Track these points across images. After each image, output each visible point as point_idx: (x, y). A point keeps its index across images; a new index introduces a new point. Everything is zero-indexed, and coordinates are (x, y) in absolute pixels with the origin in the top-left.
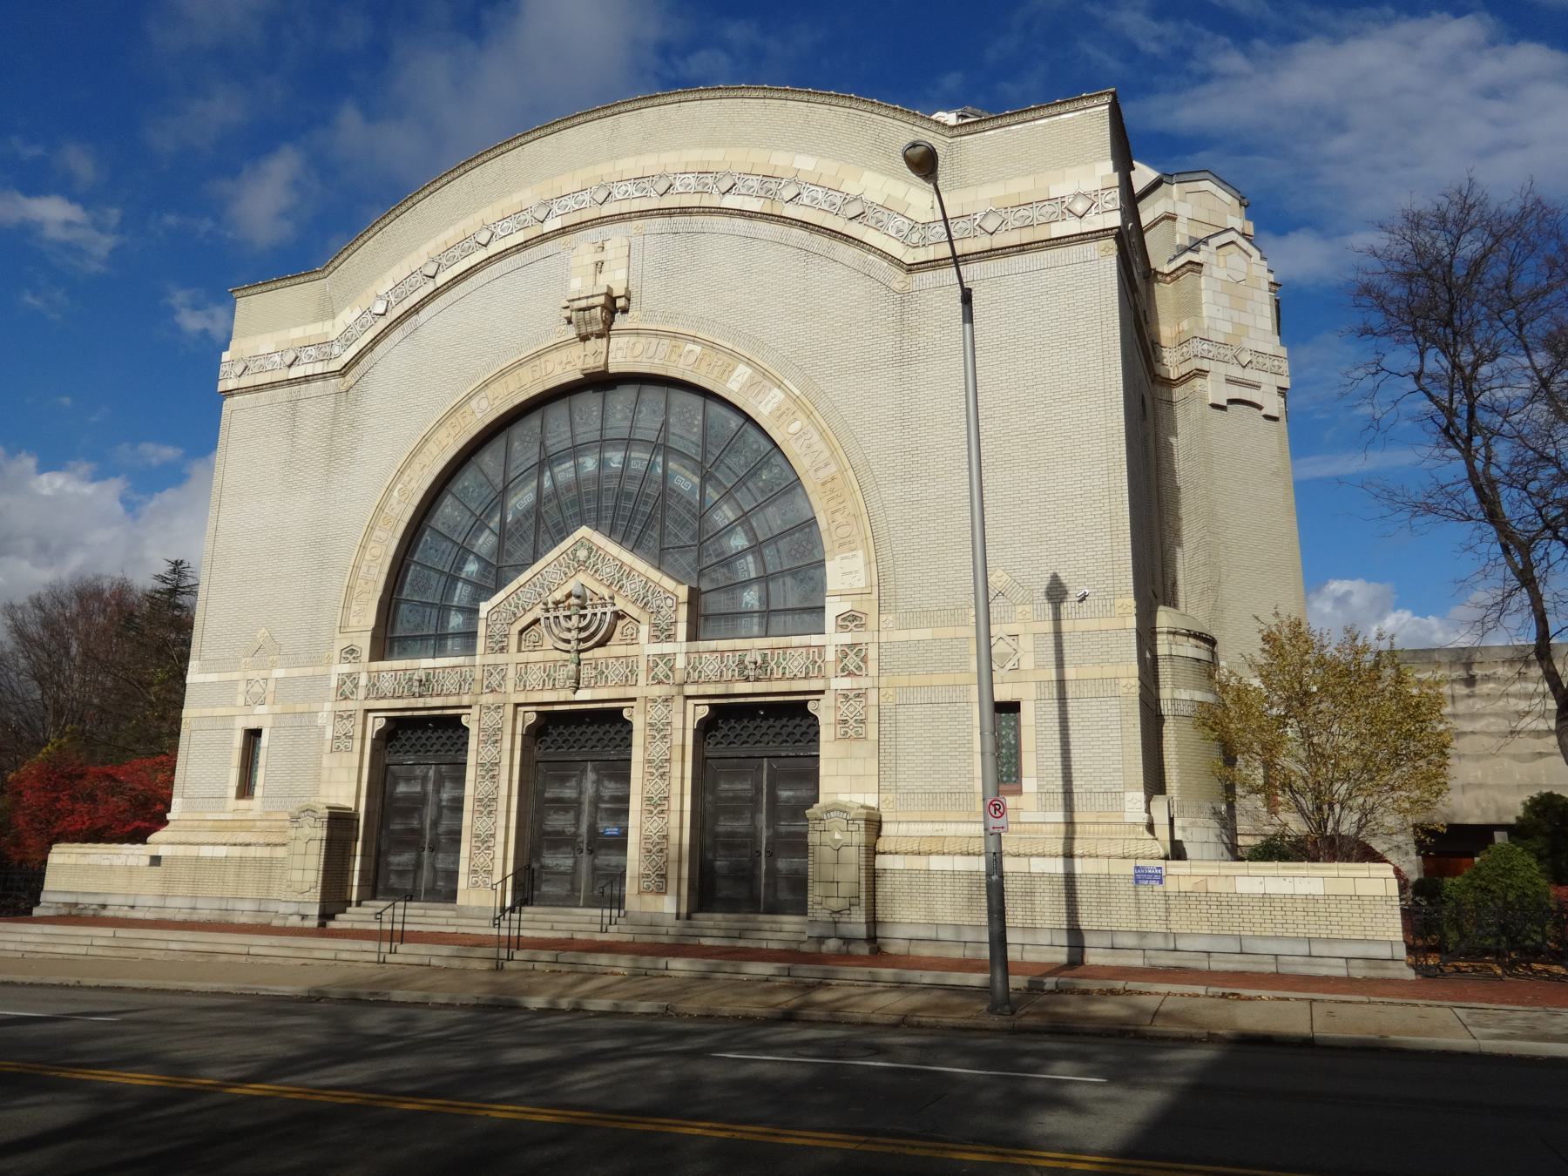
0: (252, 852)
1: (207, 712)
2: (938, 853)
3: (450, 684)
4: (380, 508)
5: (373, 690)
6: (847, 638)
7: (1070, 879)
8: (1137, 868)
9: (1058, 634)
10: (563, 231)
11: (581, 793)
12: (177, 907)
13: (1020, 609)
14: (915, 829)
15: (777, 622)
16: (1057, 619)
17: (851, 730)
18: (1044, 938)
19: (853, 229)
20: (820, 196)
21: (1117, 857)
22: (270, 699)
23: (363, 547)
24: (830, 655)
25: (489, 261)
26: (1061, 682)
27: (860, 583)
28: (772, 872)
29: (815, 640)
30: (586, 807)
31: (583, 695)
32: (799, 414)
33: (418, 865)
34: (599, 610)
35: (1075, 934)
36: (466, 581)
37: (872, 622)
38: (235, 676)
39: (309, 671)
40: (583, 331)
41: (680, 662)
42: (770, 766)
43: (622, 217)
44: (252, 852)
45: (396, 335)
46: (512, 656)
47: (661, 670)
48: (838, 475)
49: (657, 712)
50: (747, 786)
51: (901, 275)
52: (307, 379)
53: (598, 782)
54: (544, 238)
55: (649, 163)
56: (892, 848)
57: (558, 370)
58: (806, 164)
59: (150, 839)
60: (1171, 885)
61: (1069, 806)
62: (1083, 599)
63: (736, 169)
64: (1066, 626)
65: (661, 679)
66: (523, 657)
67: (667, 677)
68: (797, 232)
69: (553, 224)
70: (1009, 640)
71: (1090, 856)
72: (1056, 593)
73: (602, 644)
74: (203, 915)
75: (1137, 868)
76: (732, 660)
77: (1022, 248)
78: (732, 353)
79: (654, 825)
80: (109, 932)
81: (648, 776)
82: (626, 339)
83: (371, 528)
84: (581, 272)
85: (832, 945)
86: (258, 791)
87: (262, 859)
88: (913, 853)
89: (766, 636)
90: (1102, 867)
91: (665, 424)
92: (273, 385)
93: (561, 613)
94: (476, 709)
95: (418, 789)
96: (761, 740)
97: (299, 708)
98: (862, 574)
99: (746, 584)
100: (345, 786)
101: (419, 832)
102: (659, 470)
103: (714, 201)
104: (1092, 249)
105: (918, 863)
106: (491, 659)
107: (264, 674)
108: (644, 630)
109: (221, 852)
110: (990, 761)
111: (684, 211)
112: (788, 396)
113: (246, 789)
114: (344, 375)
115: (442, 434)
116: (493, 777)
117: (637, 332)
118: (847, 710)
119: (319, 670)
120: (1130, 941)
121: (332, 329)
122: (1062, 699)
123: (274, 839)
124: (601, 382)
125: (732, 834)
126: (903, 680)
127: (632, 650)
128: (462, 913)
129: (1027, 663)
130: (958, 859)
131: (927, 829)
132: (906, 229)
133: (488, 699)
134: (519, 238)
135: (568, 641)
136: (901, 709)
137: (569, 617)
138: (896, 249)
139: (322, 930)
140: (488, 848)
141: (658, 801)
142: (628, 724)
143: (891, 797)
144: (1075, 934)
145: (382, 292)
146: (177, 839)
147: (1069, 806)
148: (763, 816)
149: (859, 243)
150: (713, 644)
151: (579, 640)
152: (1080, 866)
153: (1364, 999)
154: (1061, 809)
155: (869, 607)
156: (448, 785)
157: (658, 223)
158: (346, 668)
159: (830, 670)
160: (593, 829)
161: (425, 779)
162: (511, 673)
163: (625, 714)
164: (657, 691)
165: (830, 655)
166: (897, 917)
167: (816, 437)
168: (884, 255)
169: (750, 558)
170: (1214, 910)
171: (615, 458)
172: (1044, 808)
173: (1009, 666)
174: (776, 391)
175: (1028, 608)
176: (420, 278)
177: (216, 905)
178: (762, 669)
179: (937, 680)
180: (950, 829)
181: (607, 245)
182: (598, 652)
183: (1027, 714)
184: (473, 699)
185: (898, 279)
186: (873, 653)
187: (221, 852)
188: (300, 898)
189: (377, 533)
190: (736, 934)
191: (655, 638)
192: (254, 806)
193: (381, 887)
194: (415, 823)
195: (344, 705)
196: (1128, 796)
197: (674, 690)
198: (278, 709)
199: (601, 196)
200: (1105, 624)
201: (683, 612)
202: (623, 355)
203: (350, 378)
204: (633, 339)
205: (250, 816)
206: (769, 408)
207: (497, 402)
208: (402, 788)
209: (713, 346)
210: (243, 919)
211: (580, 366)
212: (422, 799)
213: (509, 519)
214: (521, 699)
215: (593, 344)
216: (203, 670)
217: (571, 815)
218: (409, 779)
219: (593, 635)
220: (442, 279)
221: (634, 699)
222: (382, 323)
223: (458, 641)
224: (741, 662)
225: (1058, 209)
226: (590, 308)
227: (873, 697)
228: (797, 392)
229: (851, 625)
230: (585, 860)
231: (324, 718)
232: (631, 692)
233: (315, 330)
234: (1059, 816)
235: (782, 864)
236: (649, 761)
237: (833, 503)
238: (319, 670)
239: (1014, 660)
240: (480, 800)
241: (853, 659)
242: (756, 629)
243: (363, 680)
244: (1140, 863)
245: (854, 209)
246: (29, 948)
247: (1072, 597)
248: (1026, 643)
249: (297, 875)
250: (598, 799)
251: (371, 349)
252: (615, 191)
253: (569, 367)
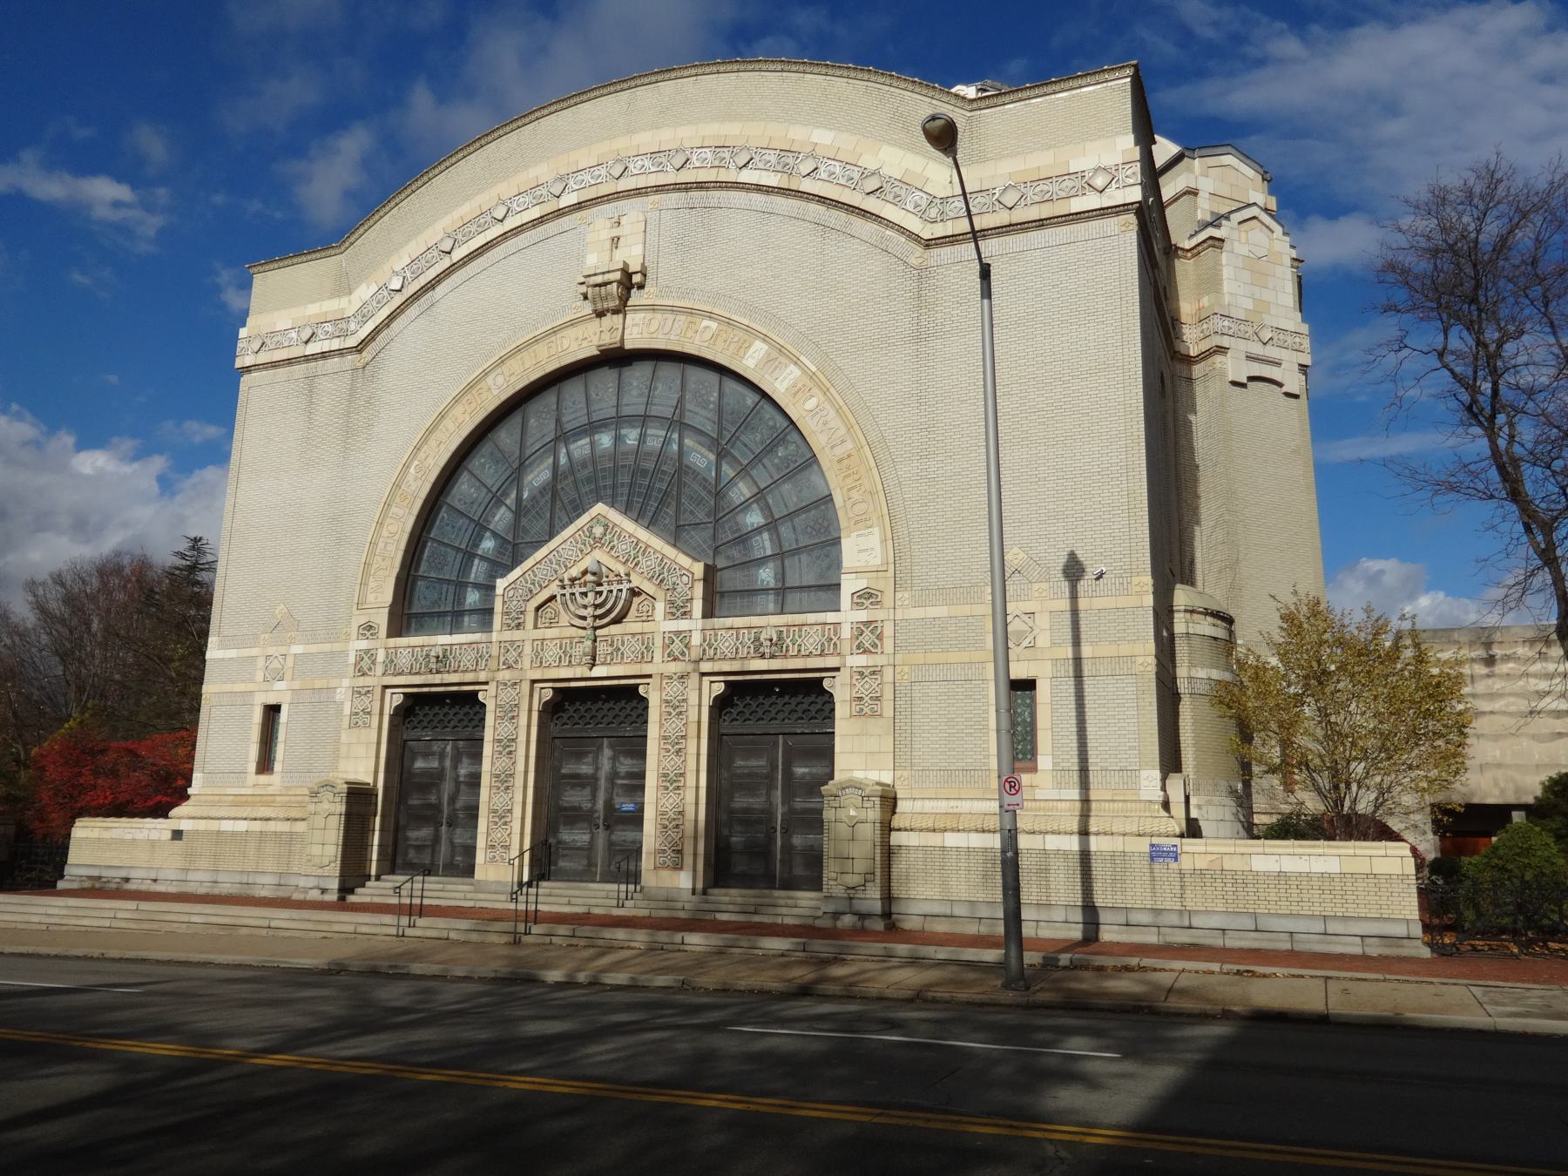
0: (272, 826)
1: (228, 687)
2: (953, 830)
3: (467, 660)
4: (397, 485)
5: (391, 666)
6: (863, 616)
7: (1085, 856)
8: (1152, 846)
9: (1075, 612)
10: (579, 206)
11: (597, 769)
12: (199, 881)
13: (1036, 586)
14: (929, 806)
15: (793, 598)
16: (1074, 597)
17: (866, 707)
18: (1059, 915)
19: (871, 204)
20: (838, 170)
21: (1131, 834)
22: (288, 676)
23: (380, 523)
24: (846, 632)
25: (505, 236)
26: (1078, 661)
27: (876, 561)
28: (788, 848)
29: (830, 617)
30: (602, 783)
31: (599, 671)
32: (815, 390)
33: (436, 839)
34: (615, 587)
35: (1090, 912)
36: (482, 558)
37: (888, 600)
38: (254, 652)
39: (327, 647)
40: (599, 307)
41: (696, 639)
42: (785, 743)
43: (639, 192)
44: (272, 826)
45: (413, 311)
46: (529, 633)
47: (677, 646)
48: (854, 452)
49: (673, 689)
50: (762, 763)
51: (919, 250)
52: (324, 355)
53: (614, 759)
54: (559, 213)
55: (666, 137)
56: (907, 825)
57: (574, 347)
58: (823, 137)
59: (172, 813)
60: (1186, 863)
61: (1084, 784)
62: (1100, 576)
63: (753, 144)
64: (1083, 603)
65: (677, 656)
66: (539, 634)
67: (683, 654)
68: (814, 208)
69: (569, 199)
70: (1025, 618)
71: (1105, 834)
72: (1074, 570)
73: (618, 620)
74: (225, 889)
75: (1152, 846)
76: (747, 637)
77: (1041, 223)
78: (748, 330)
79: (670, 802)
80: (131, 905)
81: (663, 753)
82: (641, 315)
83: (388, 504)
84: (597, 248)
85: (847, 921)
86: (278, 766)
87: (282, 833)
88: (928, 830)
89: (782, 613)
90: (1116, 844)
91: (681, 400)
92: (289, 362)
93: (577, 590)
94: (492, 686)
95: (436, 764)
96: (774, 716)
97: (318, 684)
98: (878, 551)
99: (763, 561)
100: (362, 760)
101: (437, 808)
102: (675, 447)
103: (730, 175)
104: (1112, 224)
105: (934, 839)
107: (283, 650)
108: (660, 607)
109: (242, 826)
110: (1005, 738)
111: (701, 186)
112: (804, 372)
113: (265, 764)
114: (360, 352)
115: (458, 410)
116: (510, 753)
117: (653, 308)
118: (862, 687)
119: (337, 647)
120: (1145, 918)
121: (348, 305)
122: (1078, 677)
123: (293, 814)
124: (617, 358)
125: (747, 810)
126: (919, 658)
127: (647, 627)
128: (480, 888)
129: (1043, 641)
130: (973, 836)
131: (942, 806)
132: (924, 204)
133: (505, 675)
134: (535, 213)
135: (584, 618)
136: (916, 687)
137: (585, 594)
138: (914, 224)
139: (342, 904)
140: (505, 823)
141: (674, 778)
142: (644, 700)
143: (906, 774)
144: (1090, 912)
145: (398, 268)
146: (198, 814)
147: (1084, 784)
148: (779, 792)
149: (877, 218)
150: (729, 622)
151: (595, 617)
152: (1095, 844)
153: (1380, 977)
154: (1077, 786)
155: (885, 584)
156: (465, 760)
157: (674, 198)
158: (364, 644)
159: (846, 647)
160: (609, 805)
161: (442, 756)
162: (528, 649)
163: (641, 690)
164: (673, 668)
165: (846, 632)
166: (912, 894)
167: (832, 413)
168: (902, 230)
169: (766, 536)
170: (1229, 888)
171: (631, 436)
172: (1059, 786)
173: (1025, 644)
174: (792, 367)
175: (1045, 586)
176: (435, 253)
177: (238, 878)
178: (778, 646)
179: (953, 657)
180: (965, 806)
181: (624, 220)
182: (614, 629)
183: (1043, 692)
184: (490, 675)
185: (916, 254)
186: (888, 631)
187: (242, 826)
188: (320, 872)
189: (394, 509)
190: (752, 909)
191: (671, 615)
192: (274, 781)
193: (399, 861)
194: (433, 799)
195: (362, 681)
196: (1144, 774)
197: (690, 667)
198: (297, 685)
199: (617, 171)
200: (1122, 602)
201: (699, 589)
202: (639, 331)
203: (367, 355)
204: (650, 315)
205: (270, 790)
206: (786, 384)
207: (513, 379)
208: (420, 764)
209: (729, 322)
210: (264, 893)
211: (596, 342)
212: (439, 775)
213: (526, 495)
214: (537, 675)
215: (609, 320)
216: (223, 646)
217: (587, 791)
218: (427, 755)
220: (458, 255)
221: (650, 676)
222: (398, 299)
223: (475, 617)
224: (757, 639)
225: (1078, 183)
226: (605, 284)
227: (888, 674)
228: (814, 369)
229: (867, 603)
230: (601, 835)
231: (343, 693)
232: (647, 669)
233: (331, 306)
234: (1075, 794)
235: (797, 840)
236: (665, 738)
237: (848, 481)
238: (337, 647)
239: (1030, 638)
240: (497, 776)
241: (868, 637)
242: (771, 607)
243: (381, 657)
244: (1156, 841)
245: (872, 184)
246: (53, 920)
247: (1091, 571)
248: (1042, 621)
249: (316, 850)
250: (614, 775)
251: (388, 325)
252: (631, 166)
253: (585, 344)
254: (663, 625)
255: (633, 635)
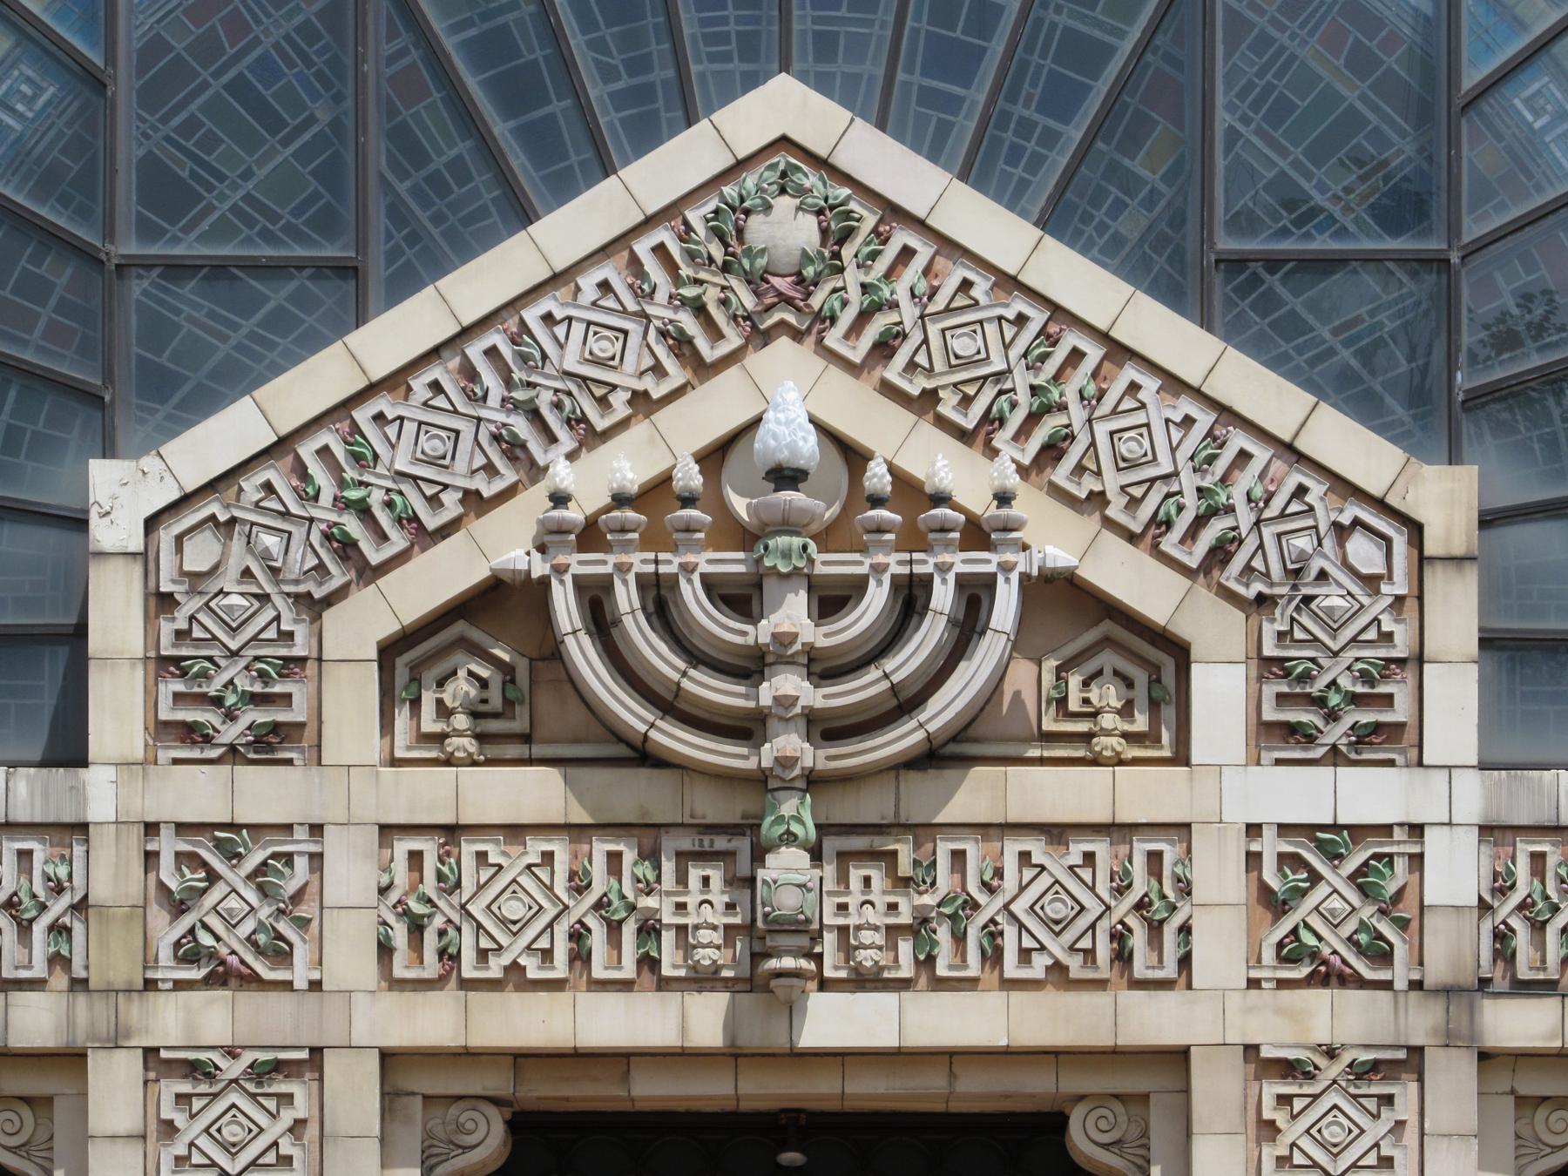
31: (833, 1021)
41: (1453, 873)
106: (200, 792)
162: (350, 874)
184: (88, 1015)
201: (1455, 616)
214: (432, 1022)
219: (905, 702)
232: (1152, 1020)
254: (1233, 786)
255: (1057, 833)
